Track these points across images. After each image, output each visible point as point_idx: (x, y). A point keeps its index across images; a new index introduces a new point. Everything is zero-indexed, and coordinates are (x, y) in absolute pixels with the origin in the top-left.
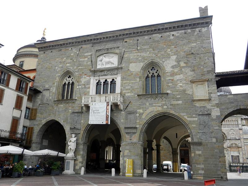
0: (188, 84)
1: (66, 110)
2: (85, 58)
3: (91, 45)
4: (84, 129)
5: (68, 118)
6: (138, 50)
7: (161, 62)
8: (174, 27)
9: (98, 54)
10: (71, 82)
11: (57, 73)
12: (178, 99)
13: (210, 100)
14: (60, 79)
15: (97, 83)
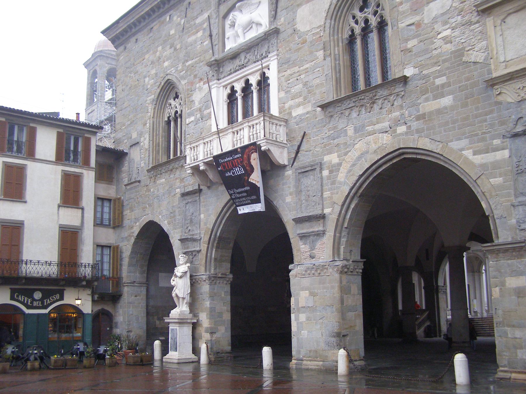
0: (470, 23)
4: (207, 238)
5: (175, 211)
14: (155, 109)
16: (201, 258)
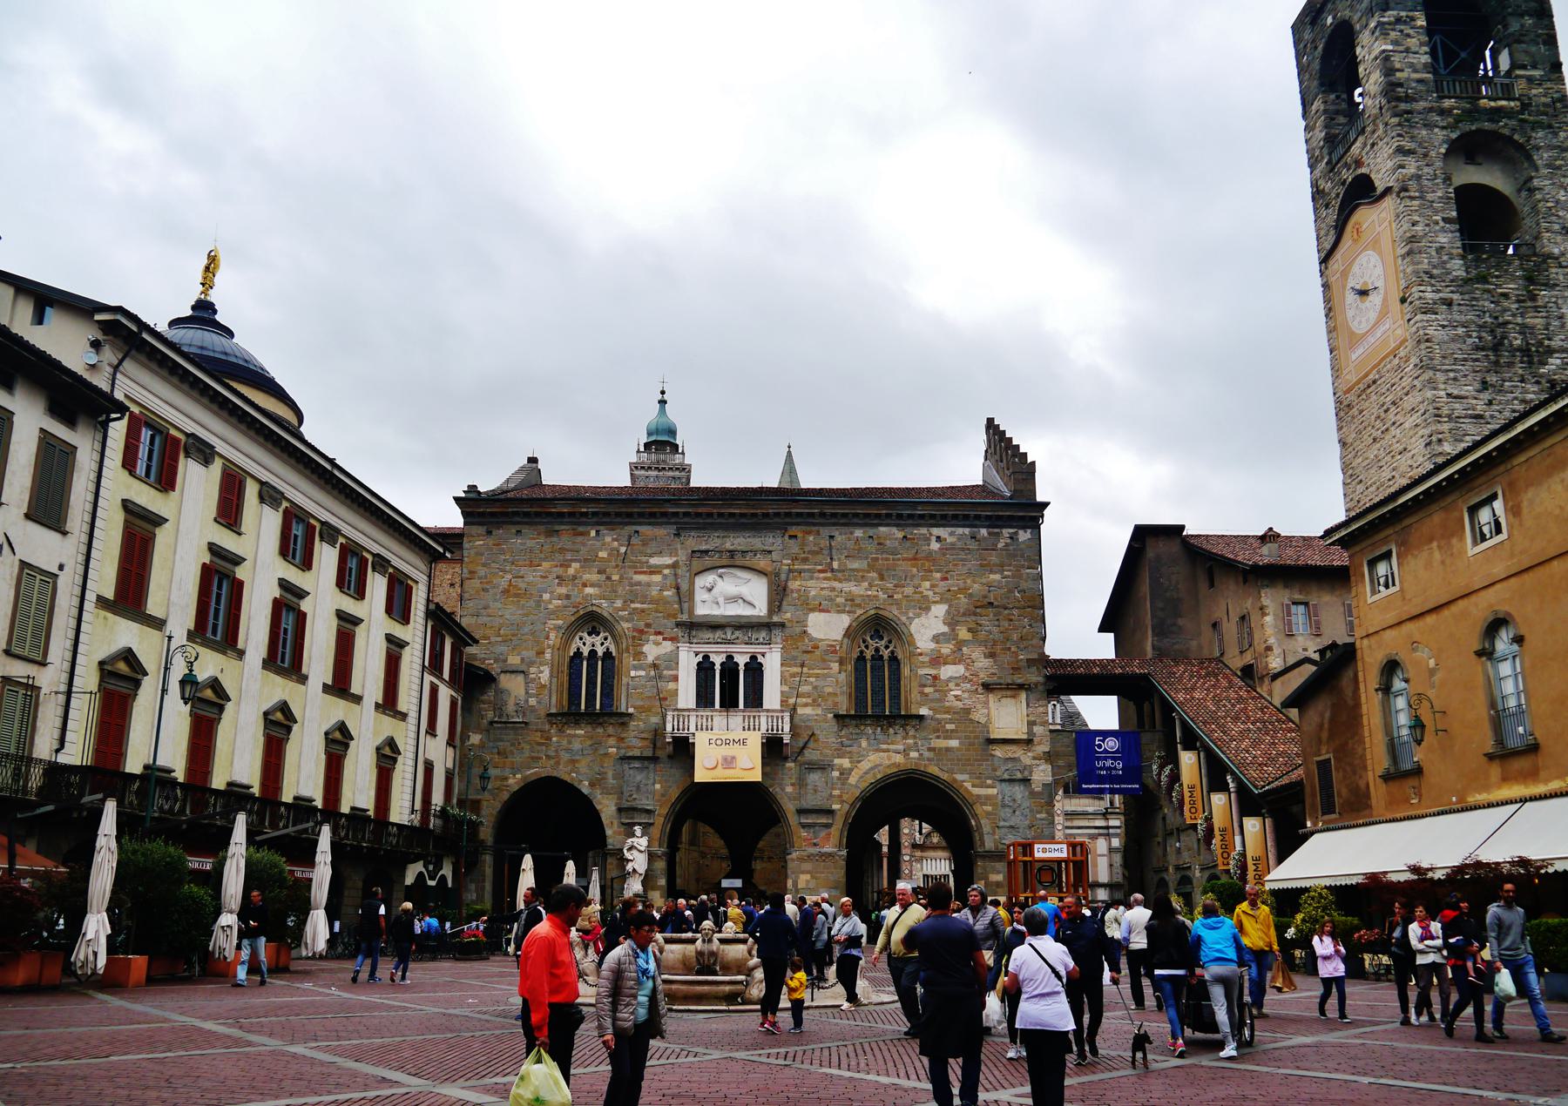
1: (596, 745)
2: (651, 573)
3: (672, 529)
6: (833, 570)
7: (904, 619)
8: (944, 517)
9: (697, 564)
10: (600, 651)
11: (554, 614)
12: (949, 735)
13: (1029, 742)
15: (699, 664)
16: (656, 831)
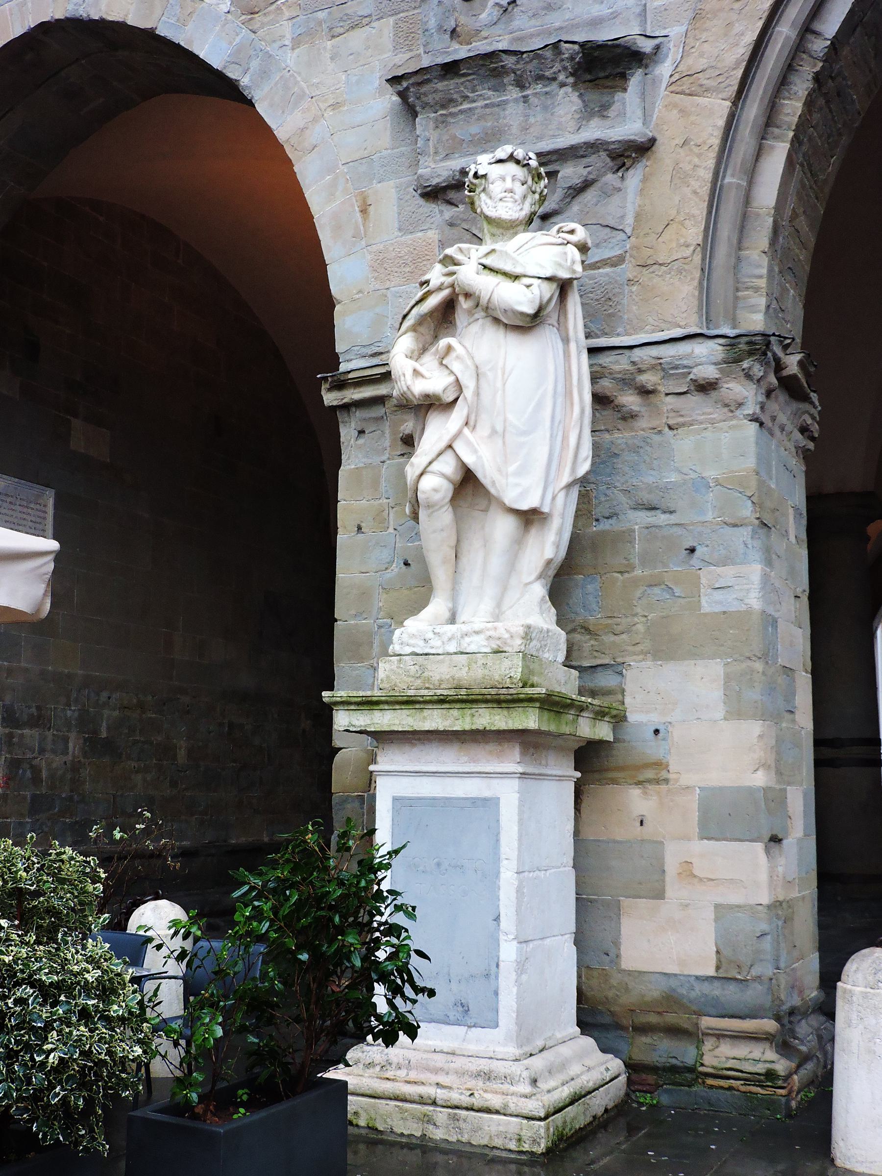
16: (671, 199)
